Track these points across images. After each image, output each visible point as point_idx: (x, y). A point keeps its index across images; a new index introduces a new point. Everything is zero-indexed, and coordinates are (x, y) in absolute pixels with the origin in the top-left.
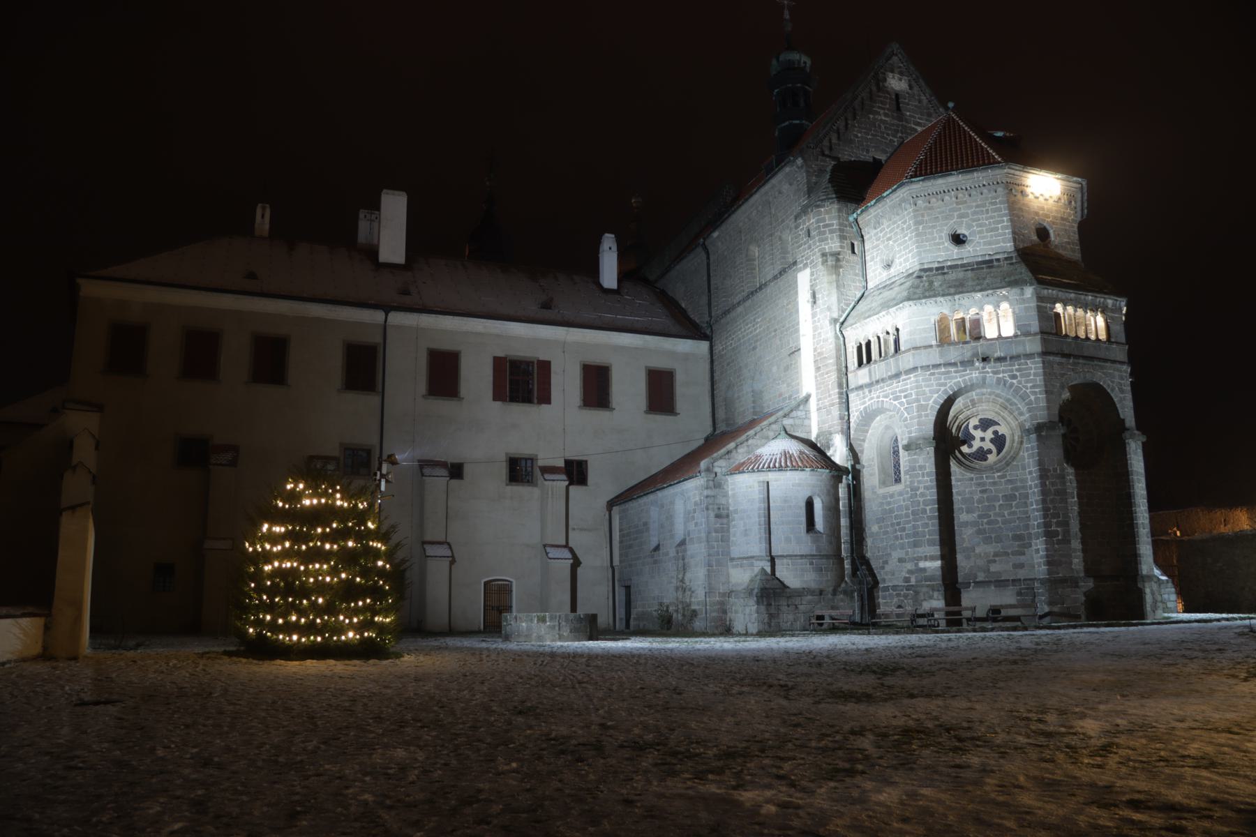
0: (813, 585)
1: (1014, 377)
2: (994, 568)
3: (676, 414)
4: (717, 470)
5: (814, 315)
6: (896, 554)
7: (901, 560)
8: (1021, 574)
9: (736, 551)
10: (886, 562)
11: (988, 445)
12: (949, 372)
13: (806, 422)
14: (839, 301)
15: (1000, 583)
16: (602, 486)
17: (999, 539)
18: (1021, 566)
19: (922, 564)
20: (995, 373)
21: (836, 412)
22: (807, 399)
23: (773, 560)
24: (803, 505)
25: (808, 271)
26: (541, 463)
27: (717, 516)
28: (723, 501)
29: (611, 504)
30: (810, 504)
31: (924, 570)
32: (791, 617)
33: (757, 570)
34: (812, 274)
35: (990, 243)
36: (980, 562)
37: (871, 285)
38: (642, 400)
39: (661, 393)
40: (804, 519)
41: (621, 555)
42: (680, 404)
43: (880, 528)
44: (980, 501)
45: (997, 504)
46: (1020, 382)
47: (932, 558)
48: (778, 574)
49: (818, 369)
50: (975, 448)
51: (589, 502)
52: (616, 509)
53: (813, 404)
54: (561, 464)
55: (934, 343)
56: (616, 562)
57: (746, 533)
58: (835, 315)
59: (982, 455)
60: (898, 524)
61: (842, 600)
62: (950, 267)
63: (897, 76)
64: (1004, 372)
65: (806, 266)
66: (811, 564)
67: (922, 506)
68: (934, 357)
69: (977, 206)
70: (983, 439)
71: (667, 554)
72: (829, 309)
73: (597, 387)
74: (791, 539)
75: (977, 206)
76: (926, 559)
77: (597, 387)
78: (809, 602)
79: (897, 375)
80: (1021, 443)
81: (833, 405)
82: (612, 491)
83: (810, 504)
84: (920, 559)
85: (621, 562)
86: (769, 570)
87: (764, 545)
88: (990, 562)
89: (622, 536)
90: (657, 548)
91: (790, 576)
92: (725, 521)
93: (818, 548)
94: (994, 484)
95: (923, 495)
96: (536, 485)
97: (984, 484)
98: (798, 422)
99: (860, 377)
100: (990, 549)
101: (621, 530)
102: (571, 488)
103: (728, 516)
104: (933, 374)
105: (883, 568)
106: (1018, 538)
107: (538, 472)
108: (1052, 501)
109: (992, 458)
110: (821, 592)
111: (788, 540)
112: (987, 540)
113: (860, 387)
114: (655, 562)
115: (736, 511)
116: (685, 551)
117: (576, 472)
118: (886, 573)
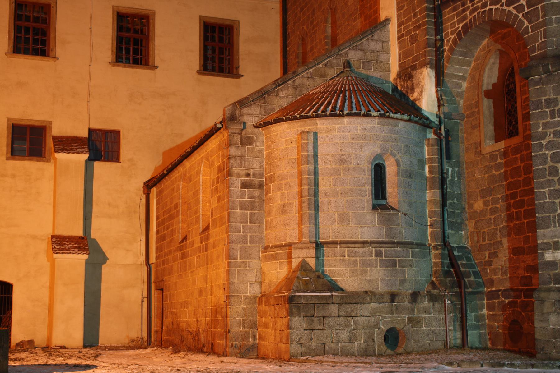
0: (382, 288)
3: (238, 76)
4: (246, 118)
10: (494, 255)
16: (139, 160)
23: (319, 246)
24: (367, 167)
26: (57, 130)
27: (245, 185)
28: (255, 165)
29: (148, 186)
30: (379, 171)
32: (345, 335)
33: (295, 263)
38: (194, 59)
40: (368, 188)
43: (486, 204)
48: (327, 269)
51: (119, 185)
52: (154, 190)
54: (85, 134)
56: (153, 260)
57: (284, 210)
61: (427, 311)
66: (379, 254)
67: (550, 163)
71: (193, 245)
74: (347, 215)
78: (373, 313)
83: (379, 171)
84: (547, 246)
85: (157, 258)
86: (312, 262)
87: (307, 227)
90: (185, 239)
92: (256, 192)
93: (389, 232)
96: (48, 161)
98: (369, 56)
101: (158, 218)
102: (97, 165)
105: (490, 263)
107: (50, 144)
110: (393, 297)
111: (344, 219)
114: (184, 256)
116: (208, 238)
117: (102, 146)
118: (495, 271)
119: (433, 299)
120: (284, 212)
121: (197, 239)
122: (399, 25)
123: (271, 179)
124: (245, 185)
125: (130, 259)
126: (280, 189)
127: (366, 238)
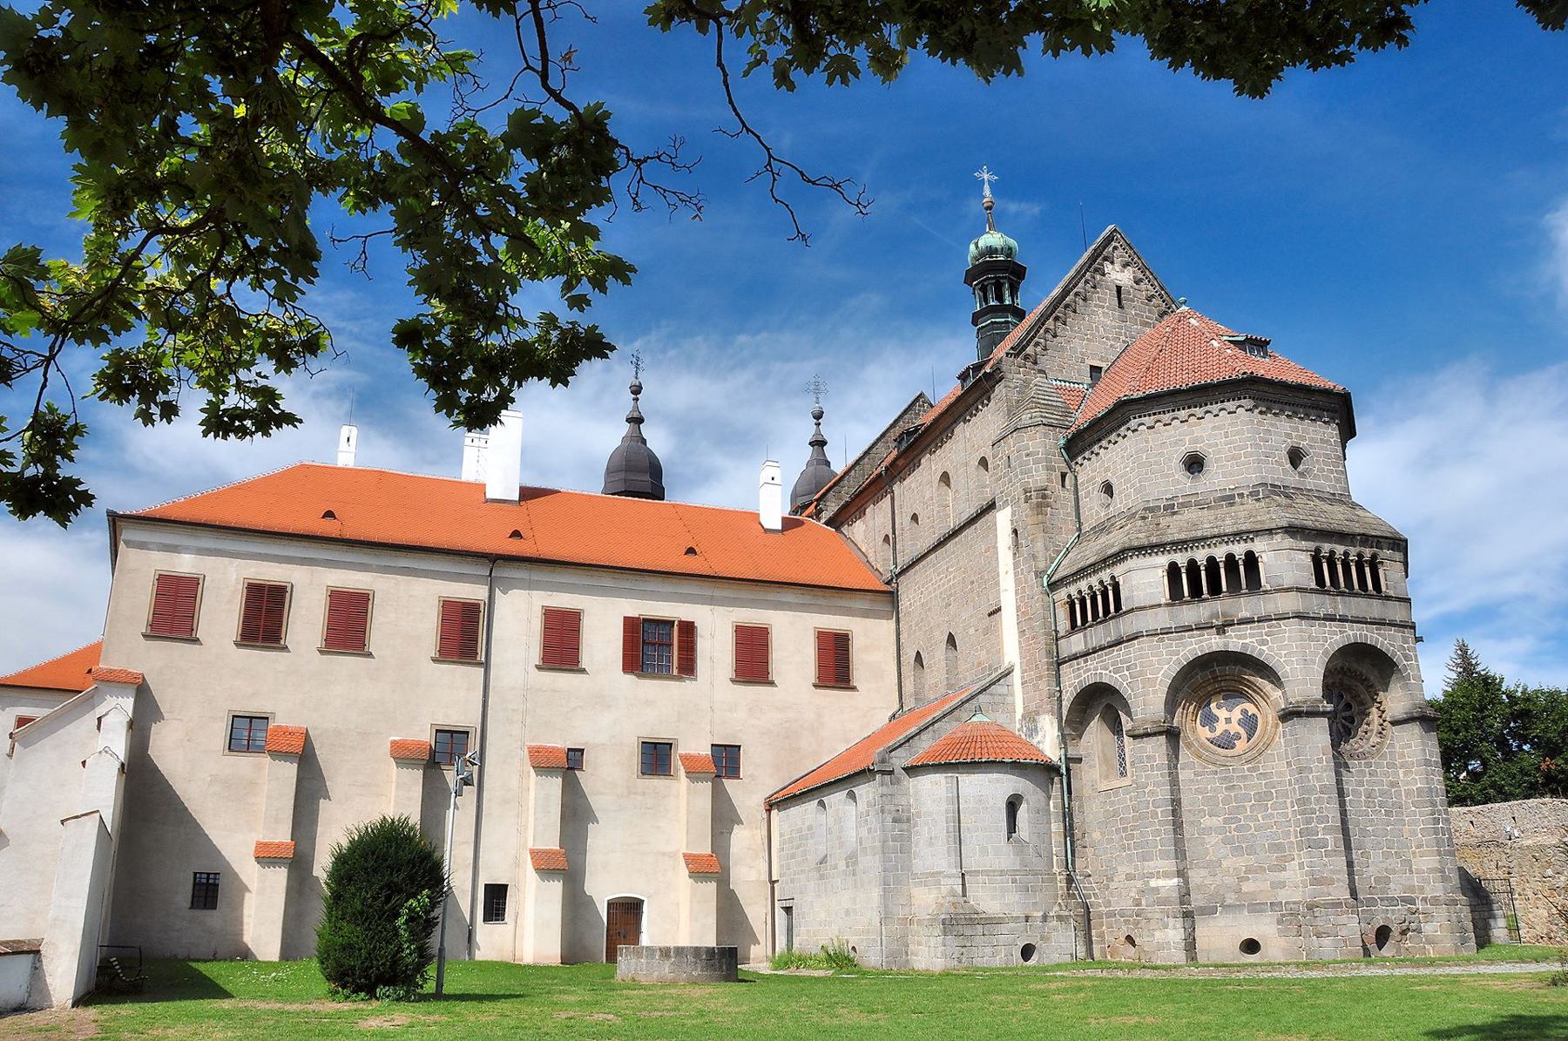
1: (1264, 642)
2: (1247, 887)
5: (1016, 566)
6: (1123, 870)
7: (1129, 877)
8: (1283, 896)
9: (919, 865)
11: (1235, 728)
12: (1181, 638)
13: (1009, 699)
14: (1047, 549)
15: (1256, 908)
17: (1251, 851)
18: (1282, 885)
19: (1153, 883)
20: (1240, 637)
21: (1045, 686)
22: (1009, 673)
25: (1008, 510)
27: (895, 821)
31: (1157, 889)
33: (945, 890)
34: (1013, 514)
35: (1232, 475)
36: (1229, 880)
37: (1086, 527)
38: (810, 671)
39: (835, 665)
41: (781, 866)
42: (858, 674)
44: (1226, 801)
45: (1248, 805)
46: (1270, 649)
47: (1166, 875)
49: (1022, 632)
50: (1218, 733)
53: (1017, 676)
55: (1163, 601)
58: (1042, 565)
59: (1226, 742)
60: (1125, 829)
62: (1183, 505)
63: (1117, 267)
64: (1252, 636)
65: (1006, 503)
68: (1162, 618)
69: (1214, 428)
70: (1228, 720)
72: (1034, 557)
73: (753, 658)
75: (1214, 428)
76: (1158, 876)
77: (753, 658)
79: (1118, 643)
80: (1277, 726)
81: (1040, 678)
82: (770, 784)
84: (1151, 875)
87: (954, 859)
88: (1241, 879)
89: (783, 843)
91: (986, 900)
92: (905, 826)
93: (1022, 860)
94: (1245, 777)
95: (1152, 793)
97: (1230, 779)
99: (1077, 643)
100: (1241, 862)
103: (908, 820)
104: (1162, 640)
106: (1277, 847)
107: (677, 763)
108: (1318, 800)
109: (1241, 745)
110: (1027, 919)
111: (984, 851)
112: (1237, 851)
113: (1075, 657)
115: (919, 815)
116: (856, 863)
119: (1060, 918)
120: (931, 844)
121: (842, 866)
122: (1023, 672)
123: (919, 815)
124: (895, 821)
125: (753, 876)
126: (926, 824)
127: (1003, 867)
